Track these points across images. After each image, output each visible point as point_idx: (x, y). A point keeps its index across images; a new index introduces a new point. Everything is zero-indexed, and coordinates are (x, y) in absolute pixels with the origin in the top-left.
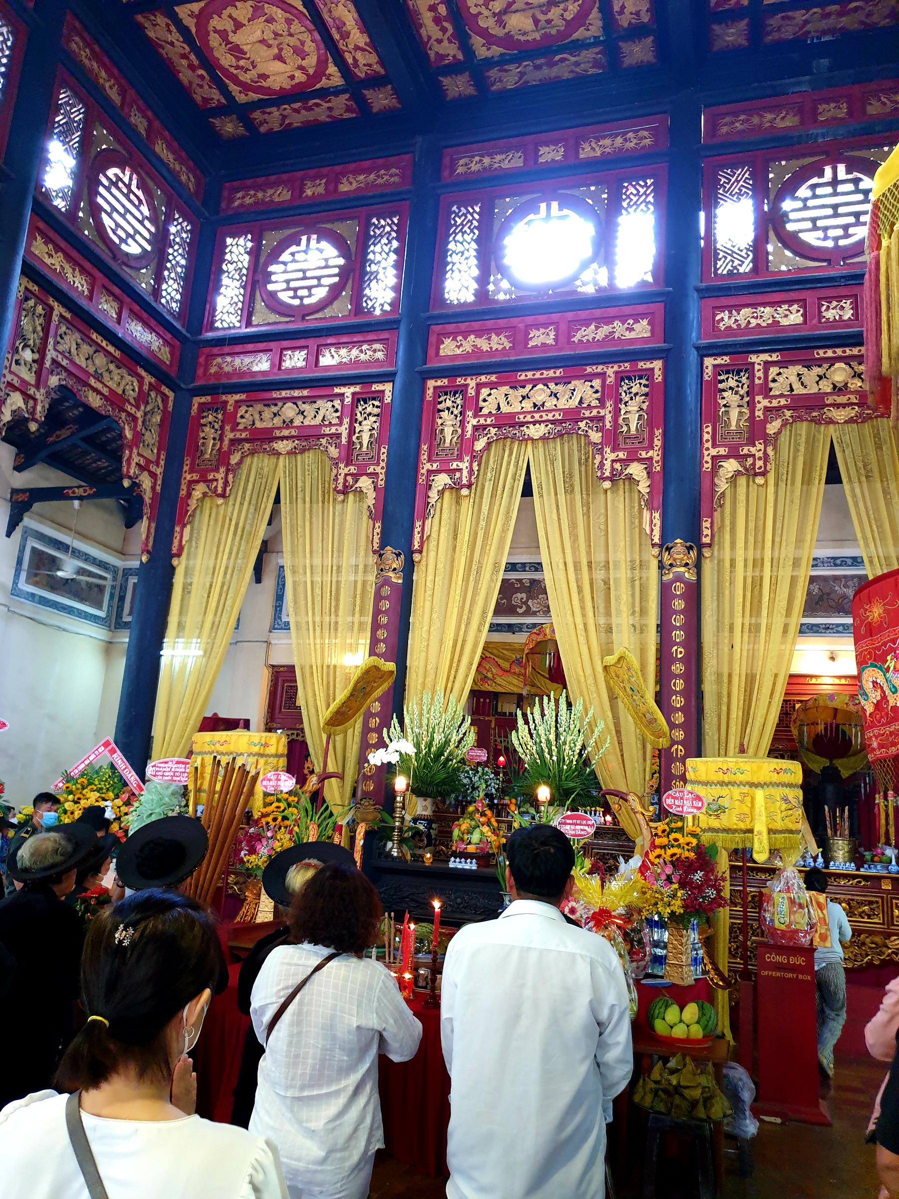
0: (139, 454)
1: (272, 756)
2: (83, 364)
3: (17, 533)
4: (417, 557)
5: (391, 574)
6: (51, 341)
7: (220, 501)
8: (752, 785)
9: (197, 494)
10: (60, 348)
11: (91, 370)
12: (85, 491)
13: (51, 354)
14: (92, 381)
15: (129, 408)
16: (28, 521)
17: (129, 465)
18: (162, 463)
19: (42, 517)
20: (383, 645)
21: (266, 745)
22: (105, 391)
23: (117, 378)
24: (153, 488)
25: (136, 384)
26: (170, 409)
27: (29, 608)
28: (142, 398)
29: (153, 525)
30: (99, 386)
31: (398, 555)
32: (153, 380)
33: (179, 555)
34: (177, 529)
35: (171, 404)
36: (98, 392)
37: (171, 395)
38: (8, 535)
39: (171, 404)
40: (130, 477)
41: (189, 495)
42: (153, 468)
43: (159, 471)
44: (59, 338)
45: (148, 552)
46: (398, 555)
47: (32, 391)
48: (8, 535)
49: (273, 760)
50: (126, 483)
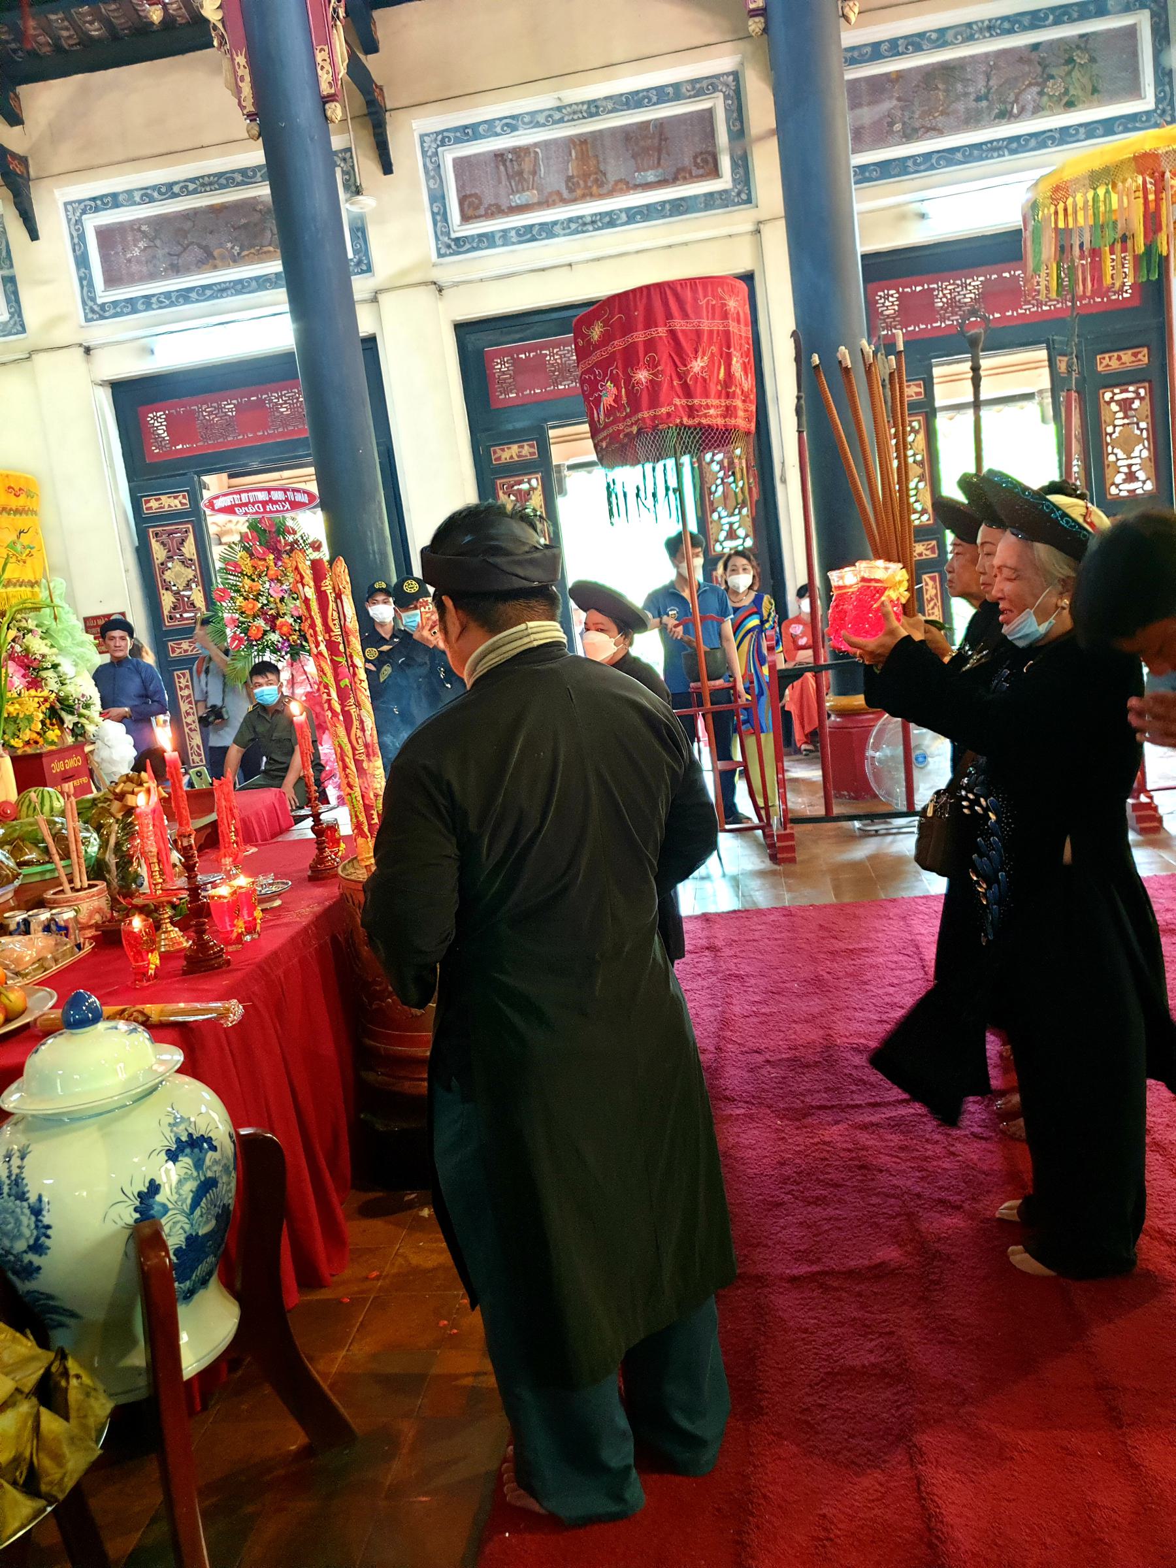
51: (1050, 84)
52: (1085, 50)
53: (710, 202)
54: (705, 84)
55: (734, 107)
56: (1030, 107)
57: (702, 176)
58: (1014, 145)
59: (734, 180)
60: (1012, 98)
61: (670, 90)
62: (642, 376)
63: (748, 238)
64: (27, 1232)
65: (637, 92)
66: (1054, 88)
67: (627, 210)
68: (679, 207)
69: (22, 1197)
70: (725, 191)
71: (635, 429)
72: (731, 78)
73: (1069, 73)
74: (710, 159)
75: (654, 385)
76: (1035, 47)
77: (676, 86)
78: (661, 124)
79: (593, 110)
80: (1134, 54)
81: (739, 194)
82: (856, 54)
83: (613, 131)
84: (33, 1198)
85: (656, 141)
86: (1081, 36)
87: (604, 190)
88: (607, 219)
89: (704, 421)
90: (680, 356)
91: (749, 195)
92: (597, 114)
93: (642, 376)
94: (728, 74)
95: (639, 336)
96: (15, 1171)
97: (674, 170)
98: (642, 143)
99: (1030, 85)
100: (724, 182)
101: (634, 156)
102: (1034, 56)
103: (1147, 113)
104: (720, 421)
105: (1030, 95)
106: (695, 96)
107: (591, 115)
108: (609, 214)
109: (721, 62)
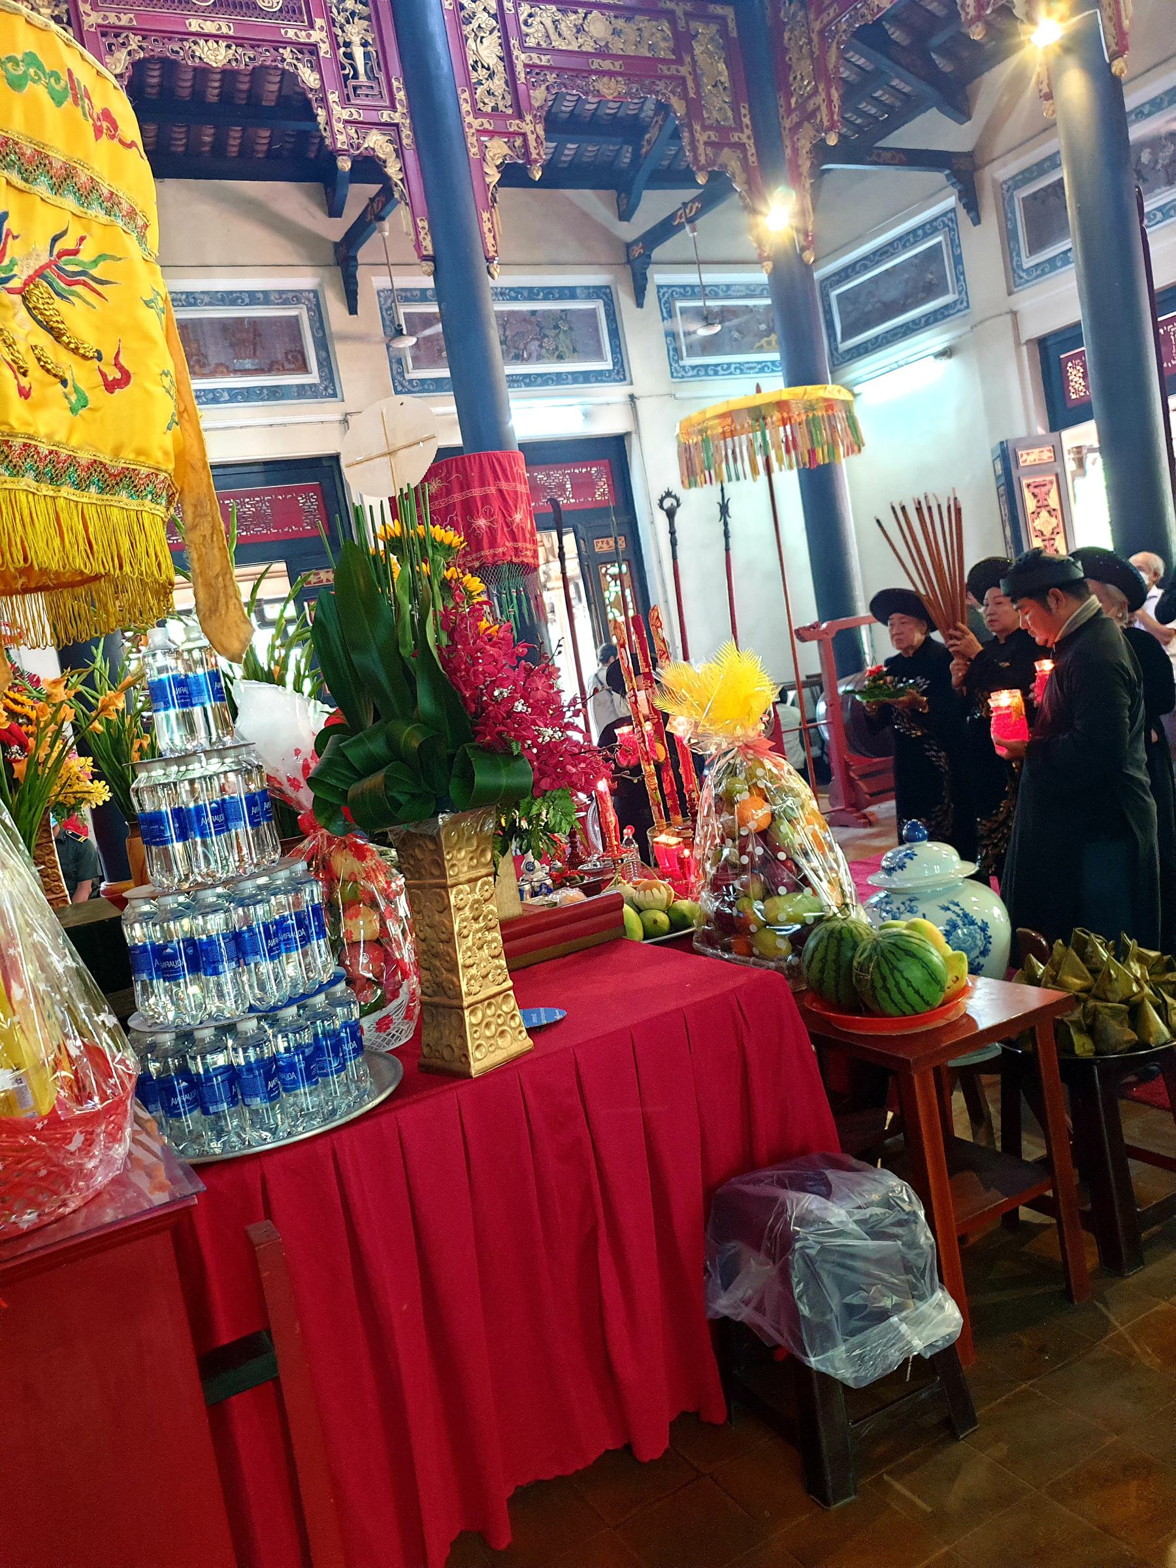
0: (705, 128)
2: (574, 47)
6: (514, 42)
10: (531, 42)
11: (589, 47)
13: (521, 59)
14: (596, 64)
15: (664, 69)
17: (694, 149)
18: (746, 120)
22: (617, 66)
23: (633, 36)
25: (665, 26)
26: (734, 34)
28: (682, 43)
30: (607, 65)
32: (688, 7)
35: (732, 25)
36: (611, 74)
37: (728, 12)
39: (732, 25)
40: (701, 169)
42: (735, 137)
43: (745, 136)
44: (523, 28)
47: (514, 125)
51: (546, 340)
52: (565, 320)
53: (302, 392)
54: (290, 295)
55: (316, 318)
56: (535, 355)
57: (293, 370)
58: (527, 380)
59: (321, 377)
60: (522, 346)
61: (260, 296)
62: (482, 522)
63: (337, 425)
64: (979, 943)
65: (231, 292)
66: (549, 343)
67: (230, 390)
68: (275, 393)
69: (973, 923)
70: (314, 385)
71: (477, 564)
72: (312, 295)
73: (557, 335)
74: (299, 356)
75: (491, 531)
76: (534, 313)
77: (266, 293)
78: (254, 322)
79: (192, 301)
80: (596, 329)
81: (326, 389)
82: (409, 294)
83: (211, 321)
84: (980, 923)
85: (251, 335)
86: (562, 311)
87: (206, 370)
88: (211, 396)
89: (525, 560)
90: (507, 510)
91: (334, 390)
92: (195, 304)
93: (482, 522)
94: (309, 291)
95: (477, 492)
96: (960, 912)
97: (268, 362)
98: (238, 336)
99: (533, 339)
100: (313, 377)
101: (232, 345)
102: (533, 319)
103: (608, 371)
104: (531, 560)
105: (534, 346)
106: (282, 304)
107: (190, 305)
108: (213, 391)
109: (304, 280)
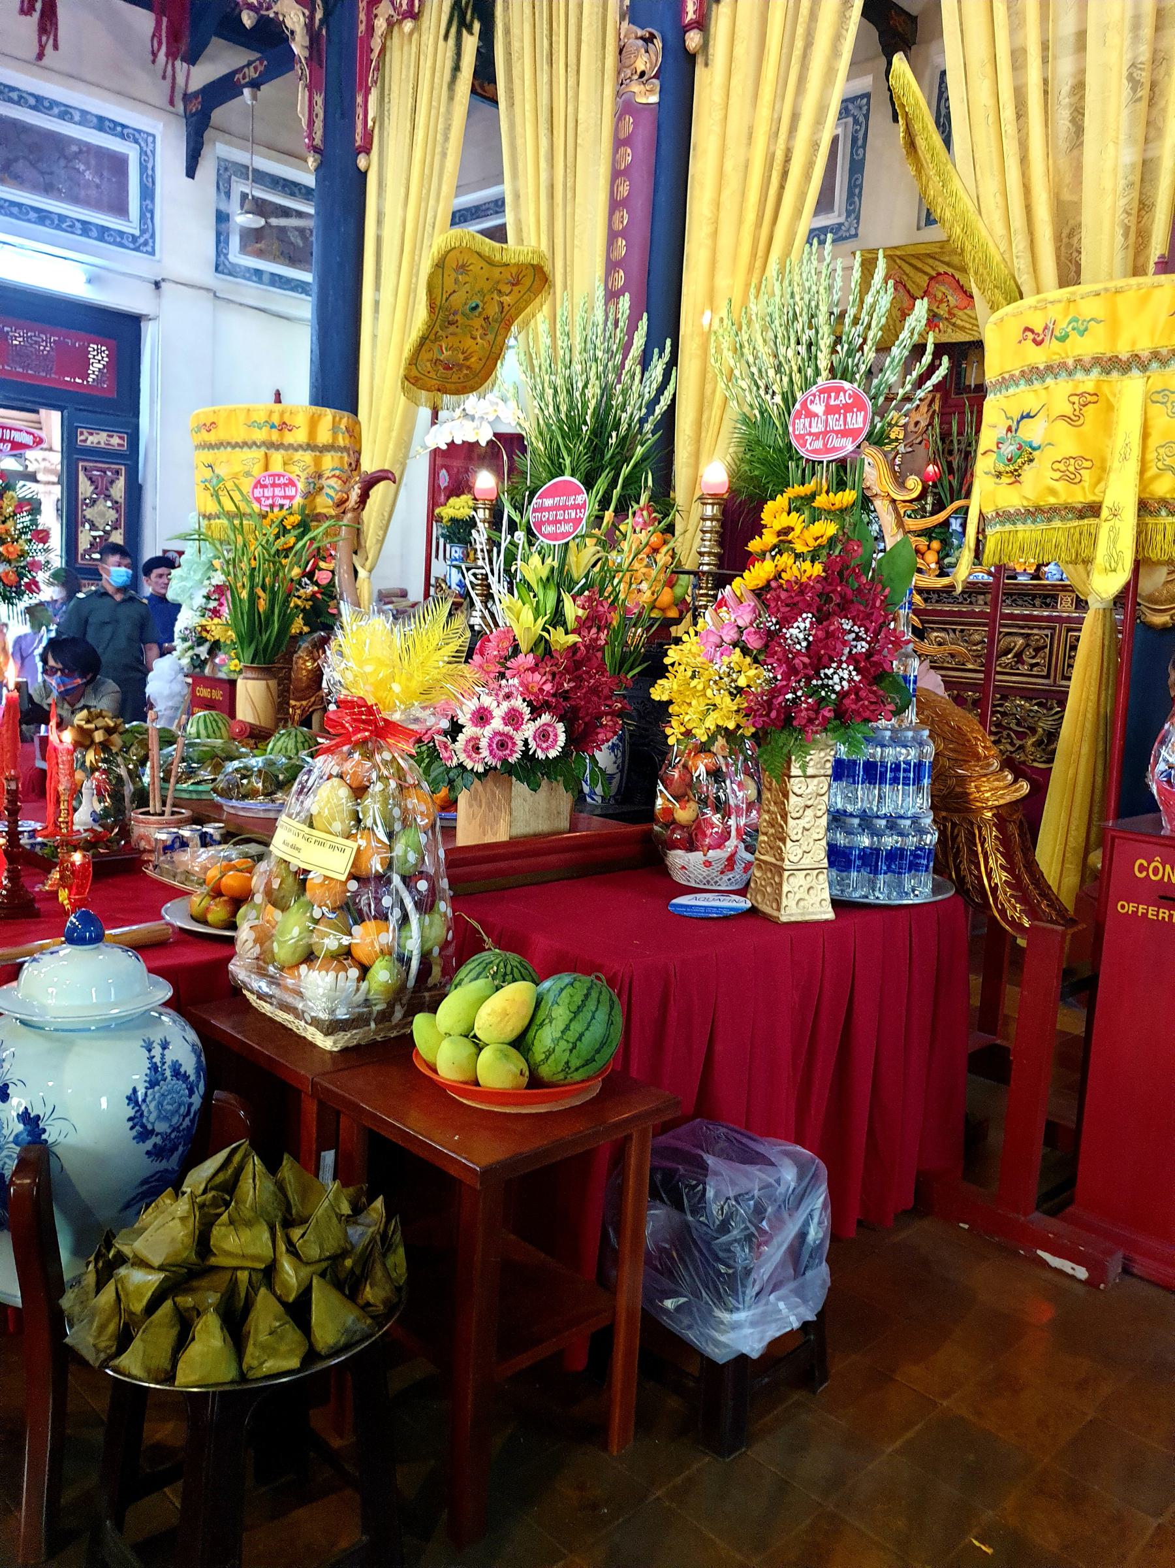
1: (299, 447)
3: (207, 169)
4: (693, 40)
5: (636, 87)
7: (408, 25)
8: (1112, 365)
9: (380, 24)
12: (256, 69)
16: (218, 150)
19: (252, 141)
20: (621, 242)
21: (283, 427)
24: (309, 26)
27: (251, 292)
29: (319, 99)
31: (648, 40)
33: (367, 150)
34: (359, 100)
38: (191, 173)
41: (371, 29)
45: (316, 150)
46: (648, 40)
48: (191, 173)
49: (307, 457)
50: (248, 19)
